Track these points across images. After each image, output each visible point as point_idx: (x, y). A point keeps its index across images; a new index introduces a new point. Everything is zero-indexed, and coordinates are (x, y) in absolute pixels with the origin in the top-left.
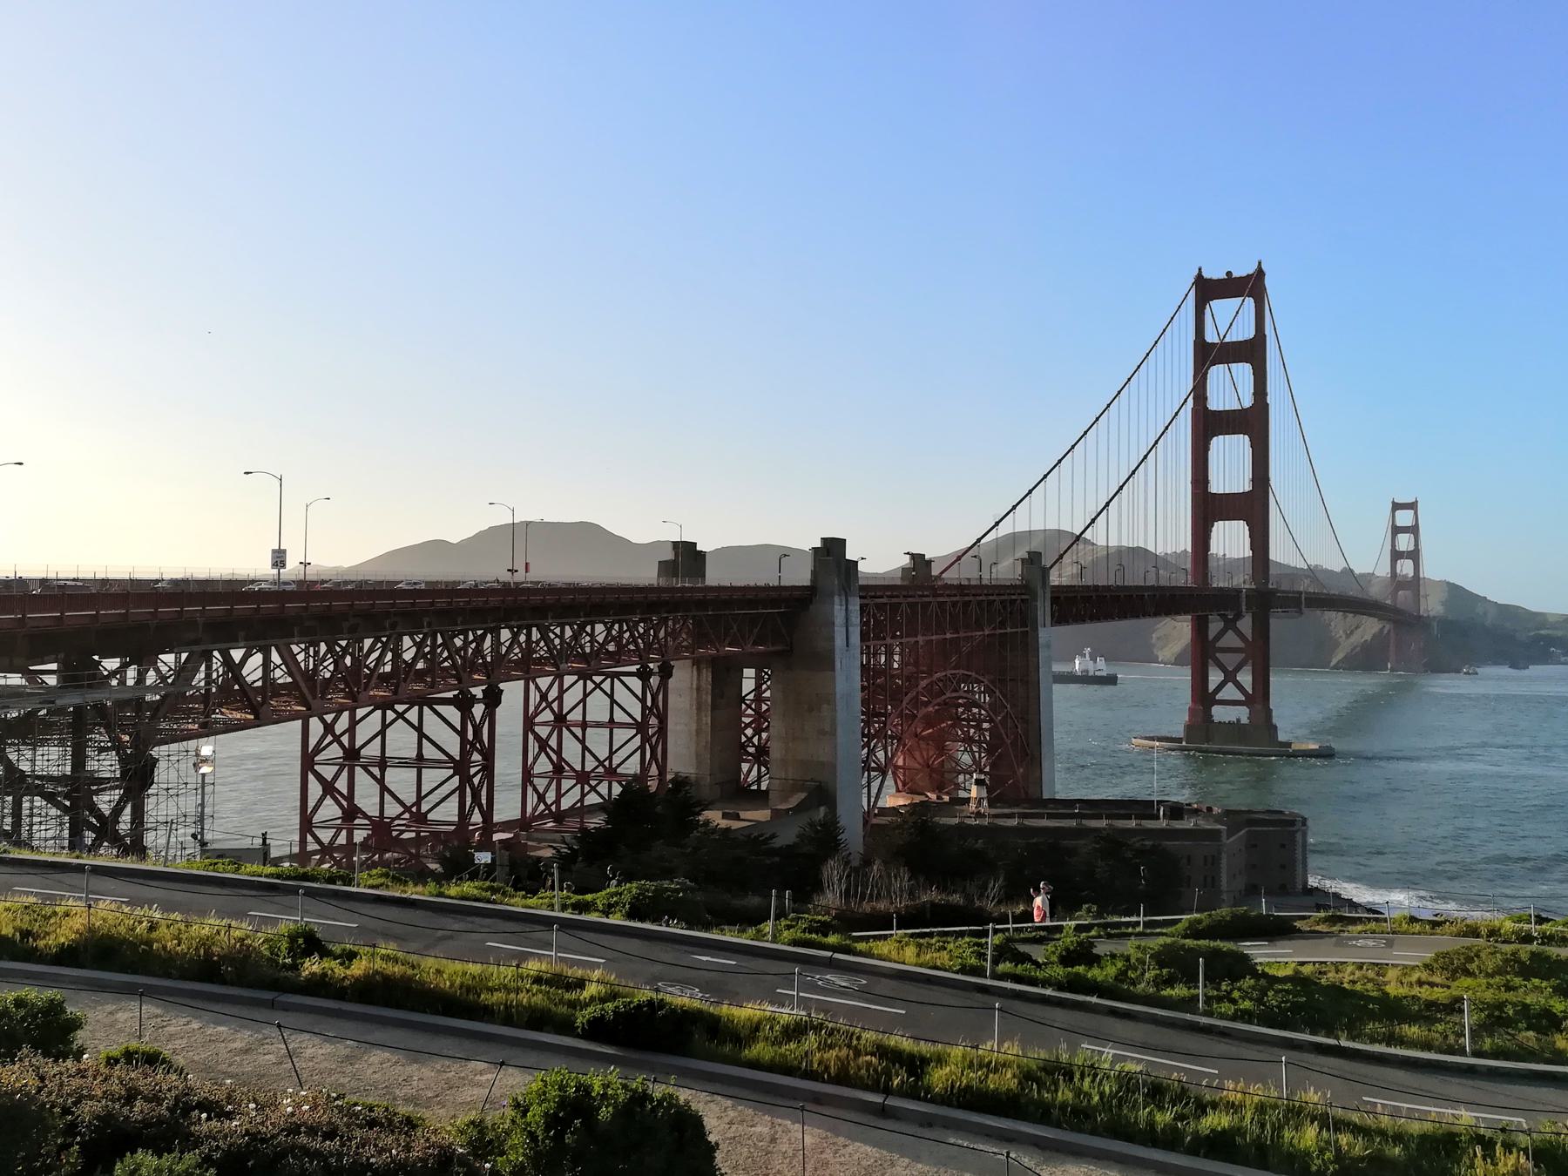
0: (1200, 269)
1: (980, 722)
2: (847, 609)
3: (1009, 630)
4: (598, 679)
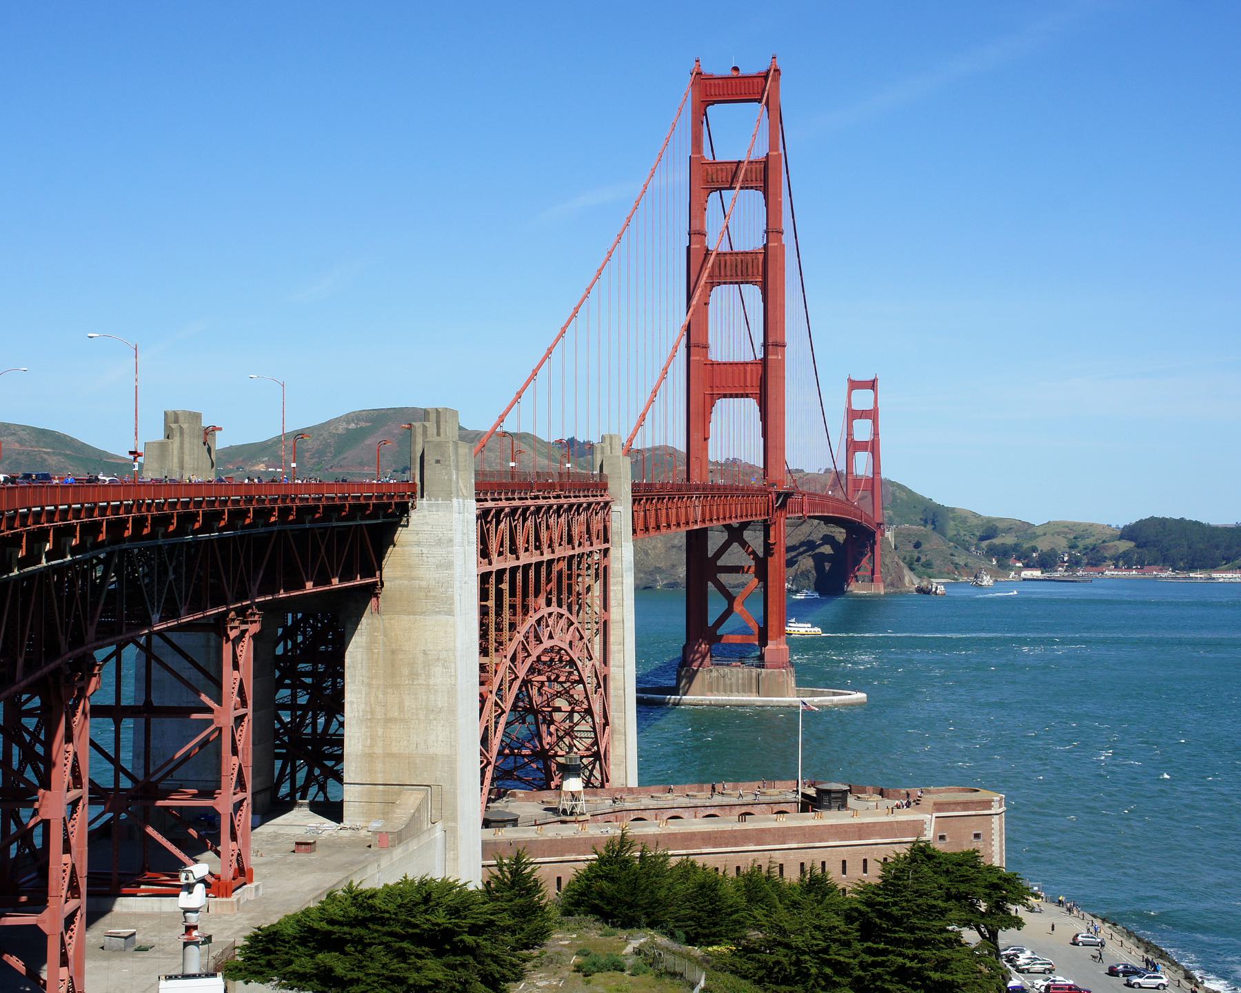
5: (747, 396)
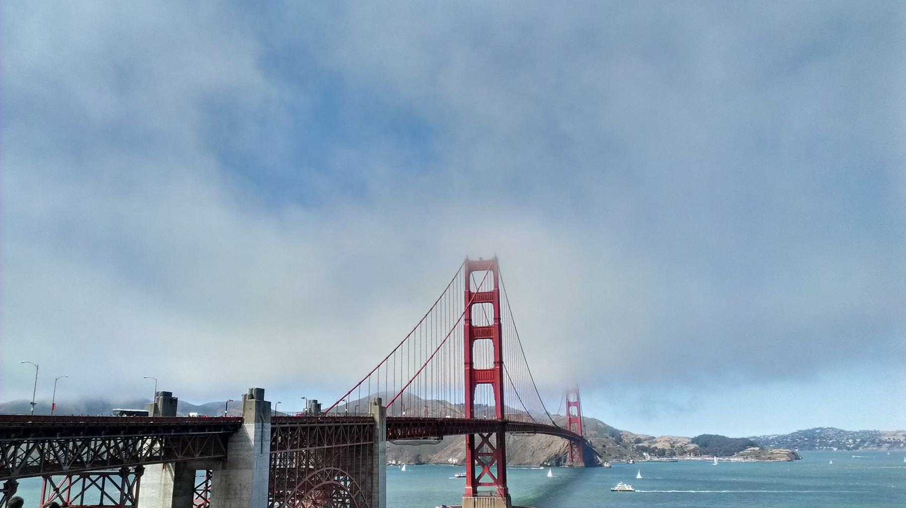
0: (467, 256)
1: (344, 499)
2: (262, 432)
3: (362, 443)
4: (94, 477)
5: (488, 383)
